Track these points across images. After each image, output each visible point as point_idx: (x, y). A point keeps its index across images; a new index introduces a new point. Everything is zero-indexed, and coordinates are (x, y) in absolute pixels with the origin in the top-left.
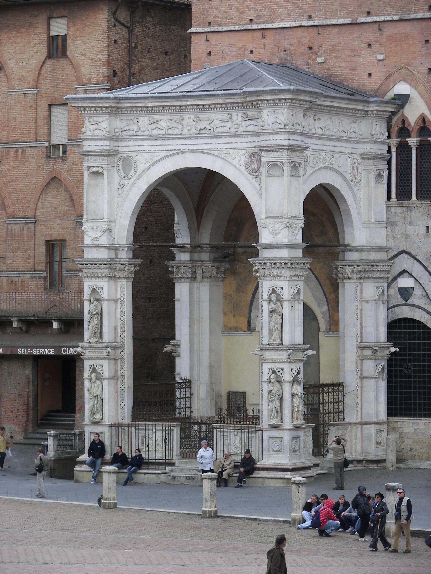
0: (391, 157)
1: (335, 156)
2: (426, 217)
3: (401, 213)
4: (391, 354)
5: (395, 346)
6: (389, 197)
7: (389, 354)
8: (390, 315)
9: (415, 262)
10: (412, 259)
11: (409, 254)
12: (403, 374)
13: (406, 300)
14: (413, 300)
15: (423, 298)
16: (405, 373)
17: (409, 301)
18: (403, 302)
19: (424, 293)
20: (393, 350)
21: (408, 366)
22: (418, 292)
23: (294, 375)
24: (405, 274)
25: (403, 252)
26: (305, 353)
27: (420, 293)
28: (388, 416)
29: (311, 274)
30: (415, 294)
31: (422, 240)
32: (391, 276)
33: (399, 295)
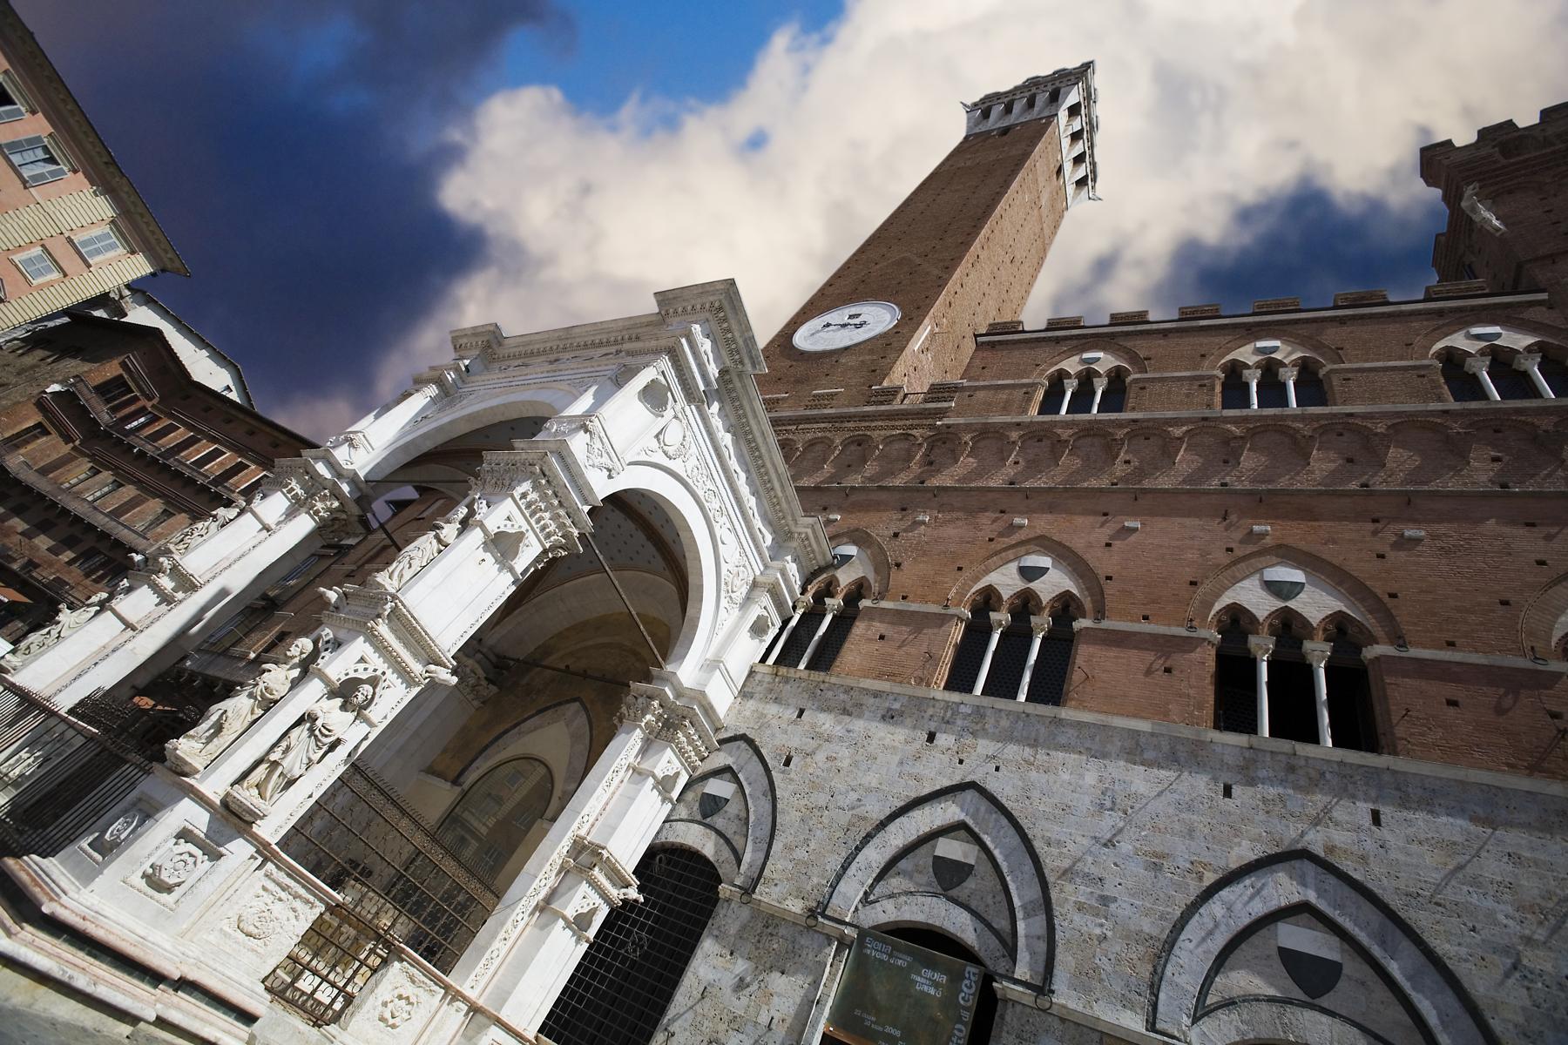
0: (792, 617)
1: (724, 517)
2: (807, 696)
3: (769, 683)
4: (625, 901)
5: (641, 889)
6: (764, 660)
7: (622, 897)
8: (664, 832)
9: (755, 758)
10: (751, 751)
11: (750, 742)
12: (623, 951)
13: (705, 817)
14: (719, 821)
15: (737, 821)
16: (626, 951)
17: (709, 819)
18: (699, 817)
19: (743, 814)
20: (633, 893)
21: (641, 939)
22: (733, 809)
23: (352, 675)
24: (728, 775)
25: (743, 737)
26: (432, 667)
27: (736, 812)
28: (541, 1031)
29: (588, 733)
30: (726, 812)
31: (783, 726)
32: (704, 768)
33: (697, 804)
